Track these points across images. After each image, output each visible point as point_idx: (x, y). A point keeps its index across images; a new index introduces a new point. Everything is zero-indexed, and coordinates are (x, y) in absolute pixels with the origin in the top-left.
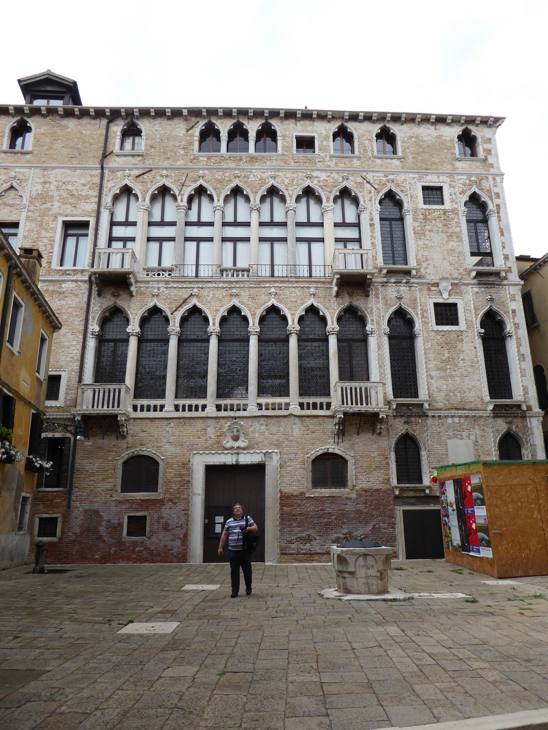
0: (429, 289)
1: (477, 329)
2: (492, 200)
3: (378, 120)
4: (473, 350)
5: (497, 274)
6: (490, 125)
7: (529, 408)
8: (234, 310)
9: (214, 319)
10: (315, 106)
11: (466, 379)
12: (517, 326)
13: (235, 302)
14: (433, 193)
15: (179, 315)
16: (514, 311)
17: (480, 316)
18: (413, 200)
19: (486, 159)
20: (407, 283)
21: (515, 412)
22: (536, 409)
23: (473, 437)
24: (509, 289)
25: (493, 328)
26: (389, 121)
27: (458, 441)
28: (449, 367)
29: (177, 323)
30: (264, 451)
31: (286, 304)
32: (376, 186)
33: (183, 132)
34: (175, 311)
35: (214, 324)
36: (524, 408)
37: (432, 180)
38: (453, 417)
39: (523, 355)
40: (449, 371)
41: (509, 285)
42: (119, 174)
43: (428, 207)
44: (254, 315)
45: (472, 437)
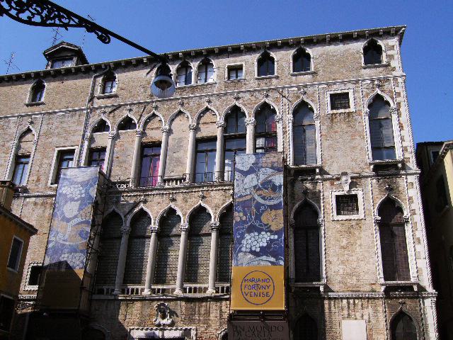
0: (332, 184)
1: (374, 215)
2: (392, 98)
3: (294, 44)
4: (370, 238)
5: (394, 165)
6: (393, 34)
7: (422, 289)
8: (171, 212)
9: (155, 220)
10: (241, 42)
11: (362, 263)
12: (413, 212)
13: (173, 205)
14: (339, 100)
15: (130, 217)
16: (410, 198)
17: (377, 205)
18: (321, 106)
19: (389, 65)
20: (312, 180)
21: (416, 293)
22: (430, 289)
23: (366, 317)
24: (406, 178)
25: (390, 213)
26: (303, 44)
27: (352, 322)
28: (346, 252)
29: (128, 224)
30: (184, 328)
31: (210, 206)
32: (290, 99)
33: (145, 74)
34: (128, 214)
35: (155, 223)
36: (415, 288)
37: (338, 89)
38: (348, 298)
39: (419, 239)
40: (346, 256)
41: (407, 175)
42: (98, 111)
43: (335, 111)
44: (184, 215)
45: (365, 317)
